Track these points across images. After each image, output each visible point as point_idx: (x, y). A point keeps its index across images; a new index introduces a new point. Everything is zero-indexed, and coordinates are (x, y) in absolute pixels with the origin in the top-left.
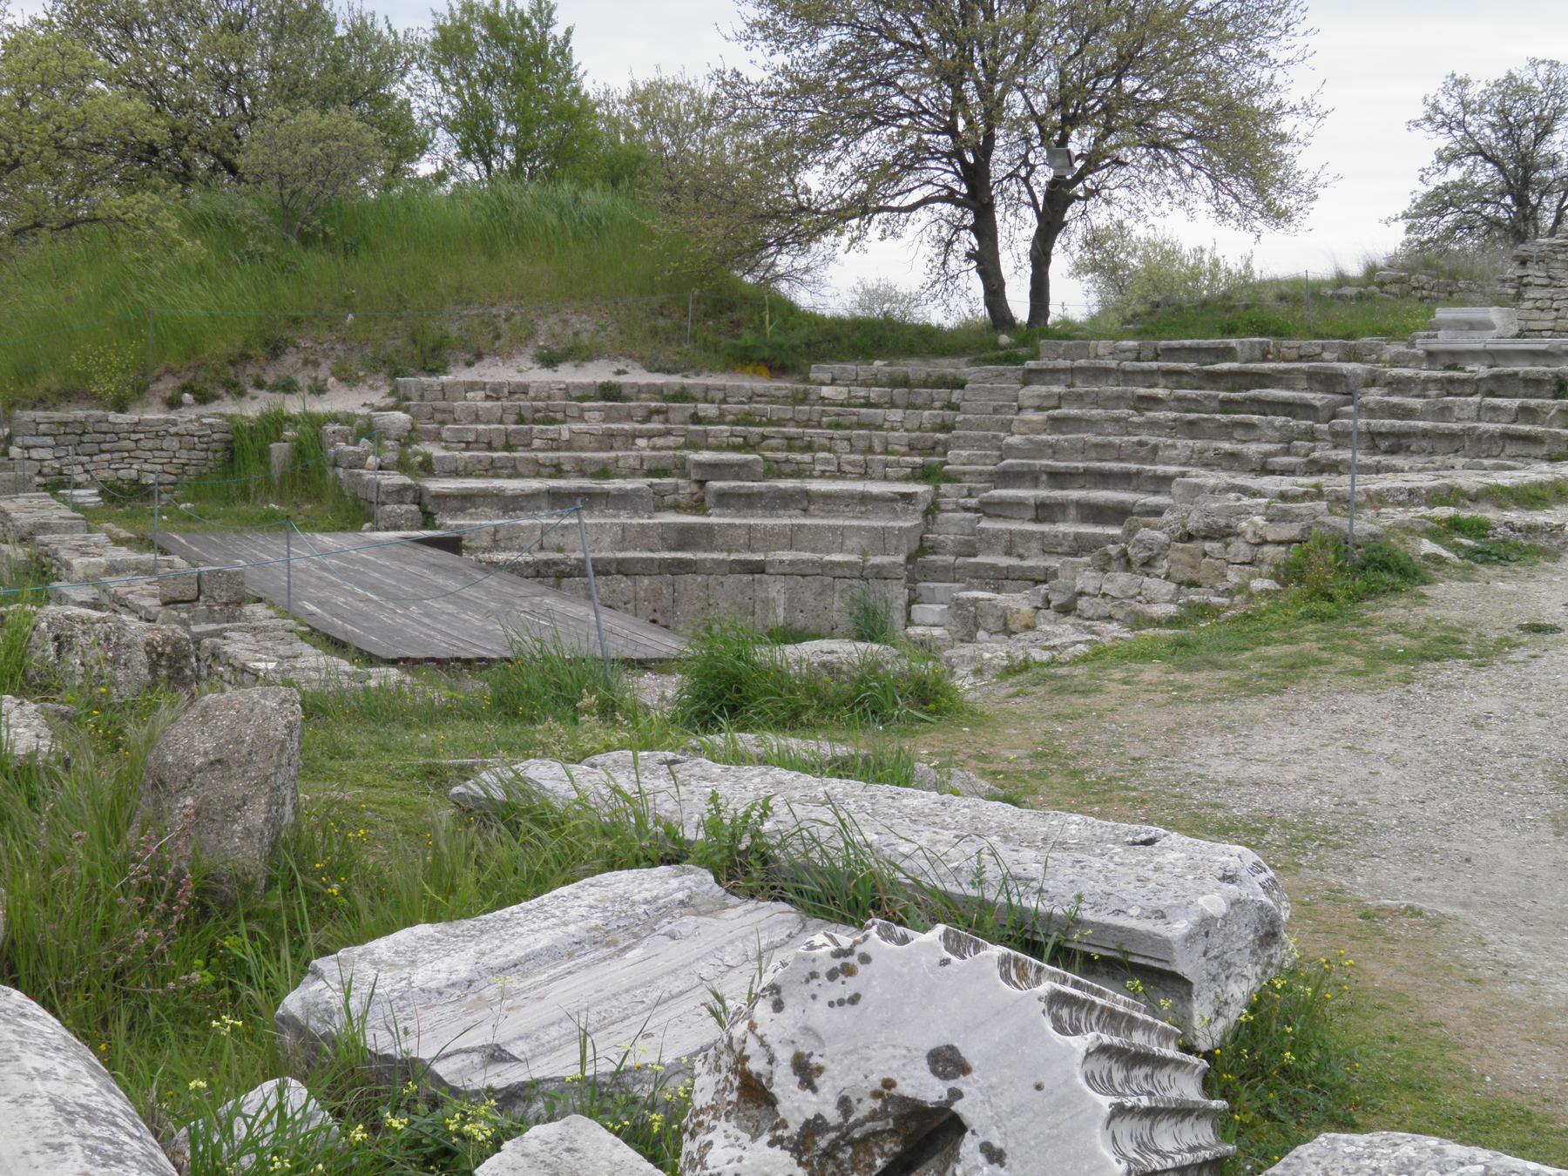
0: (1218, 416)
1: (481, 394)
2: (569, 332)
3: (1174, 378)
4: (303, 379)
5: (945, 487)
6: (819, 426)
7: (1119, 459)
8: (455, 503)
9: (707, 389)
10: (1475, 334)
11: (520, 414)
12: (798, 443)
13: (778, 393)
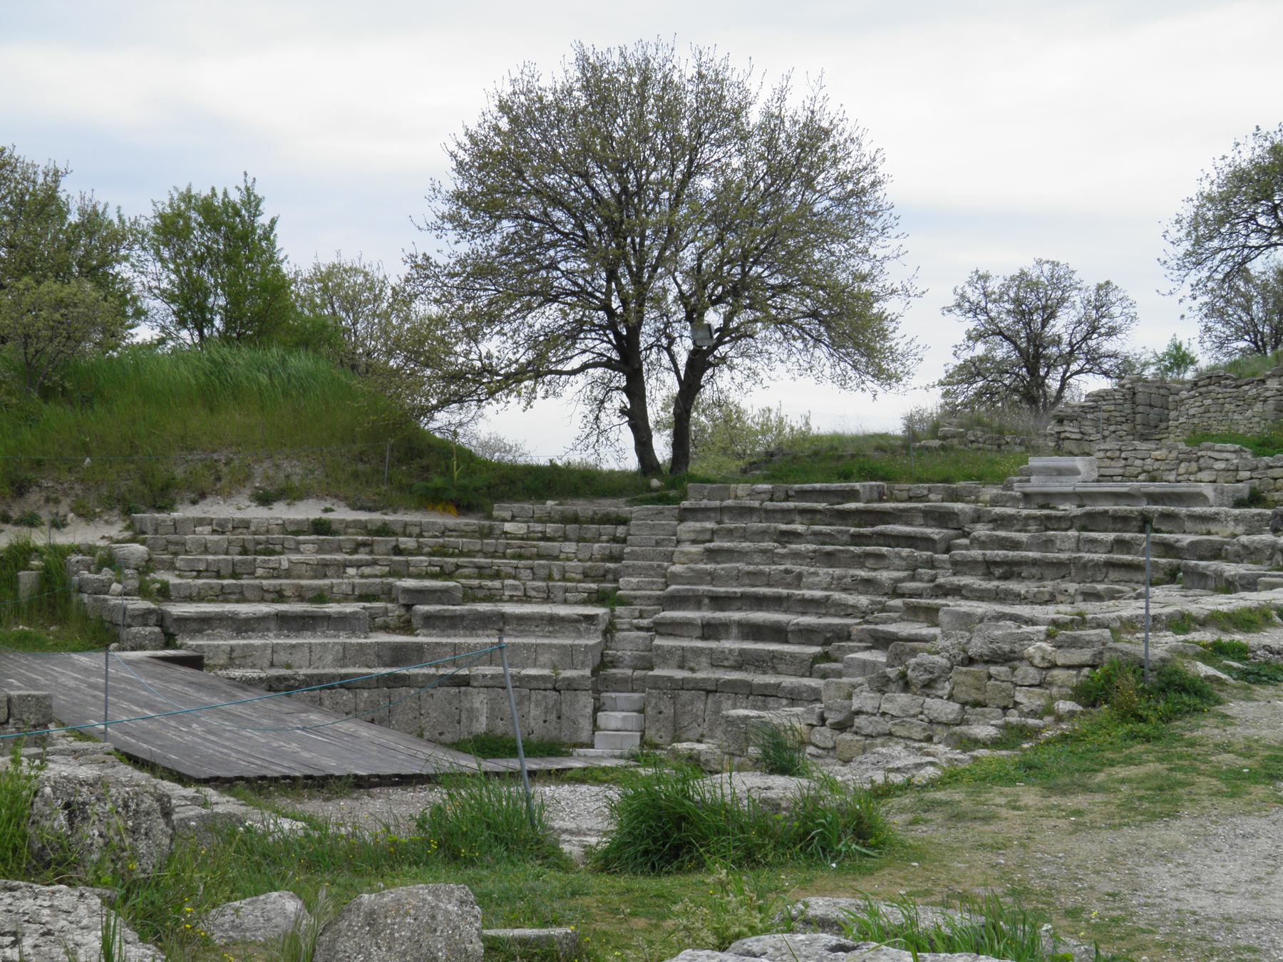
0: (852, 548)
1: (209, 528)
2: (282, 475)
4: (45, 515)
5: (619, 610)
6: (504, 556)
8: (194, 626)
9: (406, 525)
10: (1063, 479)
11: (243, 546)
12: (488, 571)
13: (466, 528)
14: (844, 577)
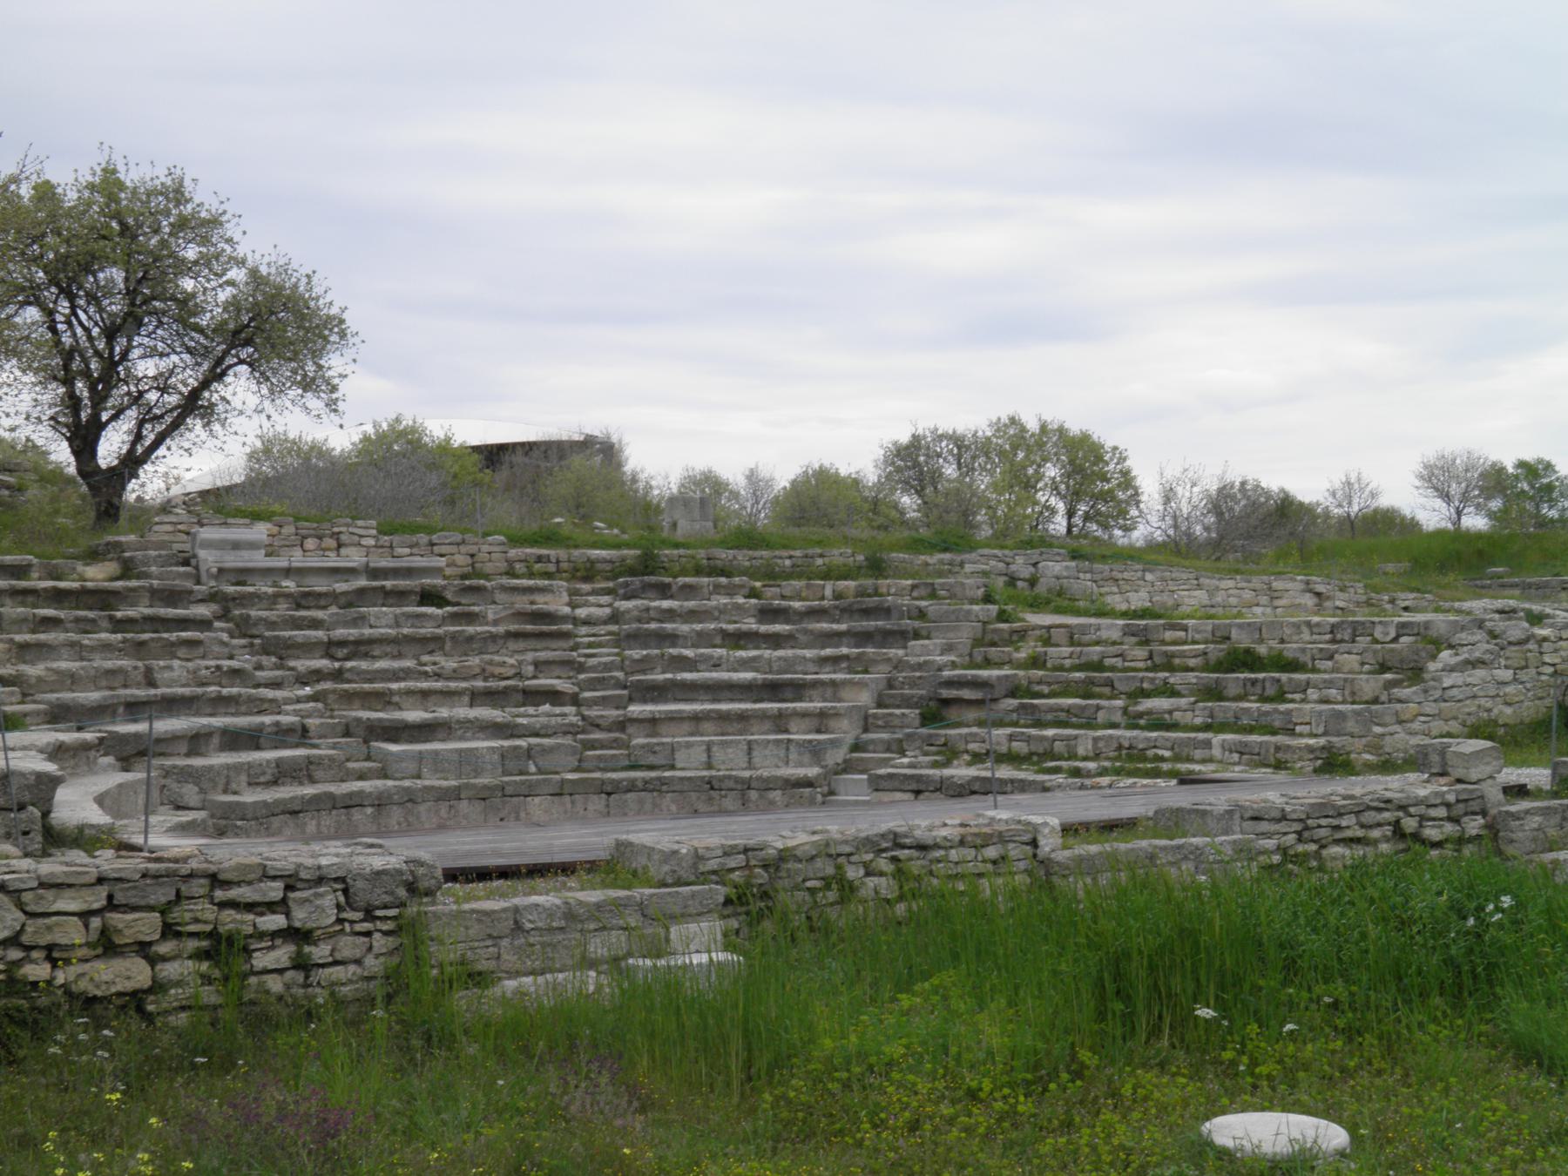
3: (20, 598)
10: (239, 553)
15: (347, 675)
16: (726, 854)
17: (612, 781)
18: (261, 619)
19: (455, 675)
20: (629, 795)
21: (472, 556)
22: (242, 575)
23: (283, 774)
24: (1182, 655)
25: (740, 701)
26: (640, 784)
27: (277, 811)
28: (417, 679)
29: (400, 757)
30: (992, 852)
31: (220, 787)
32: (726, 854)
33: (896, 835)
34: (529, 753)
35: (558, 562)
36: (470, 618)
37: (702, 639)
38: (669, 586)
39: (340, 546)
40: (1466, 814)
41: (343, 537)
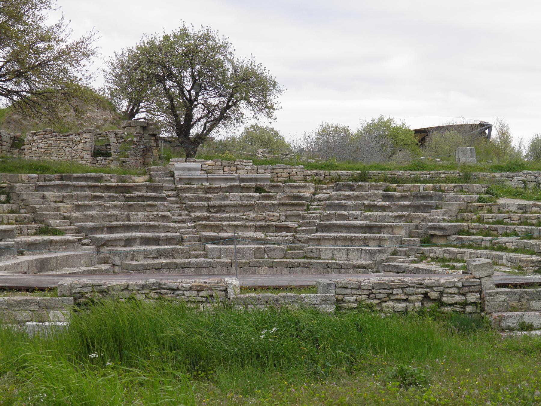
0: (141, 203)
3: (92, 189)
7: (117, 221)
10: (190, 172)
14: (150, 215)
15: (211, 219)
16: (83, 287)
17: (292, 263)
18: (186, 197)
19: (254, 220)
20: (298, 269)
21: (289, 173)
22: (190, 181)
23: (159, 254)
24: (530, 218)
25: (359, 233)
26: (302, 264)
27: (148, 268)
28: (239, 221)
29: (212, 250)
30: (204, 293)
31: (129, 258)
32: (83, 287)
33: (160, 284)
34: (265, 250)
35: (325, 176)
36: (270, 198)
37: (356, 207)
38: (353, 186)
39: (237, 169)
40: (470, 292)
41: (238, 166)
